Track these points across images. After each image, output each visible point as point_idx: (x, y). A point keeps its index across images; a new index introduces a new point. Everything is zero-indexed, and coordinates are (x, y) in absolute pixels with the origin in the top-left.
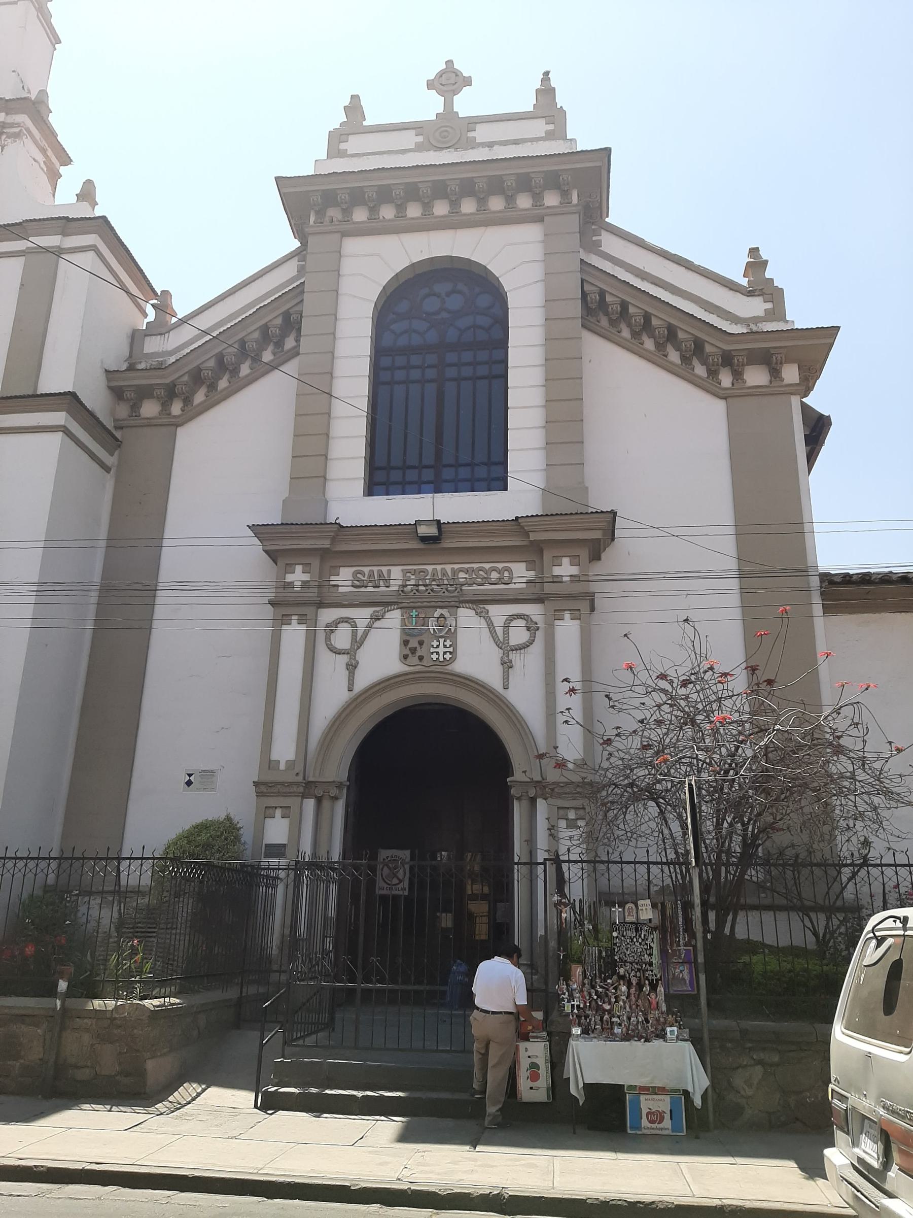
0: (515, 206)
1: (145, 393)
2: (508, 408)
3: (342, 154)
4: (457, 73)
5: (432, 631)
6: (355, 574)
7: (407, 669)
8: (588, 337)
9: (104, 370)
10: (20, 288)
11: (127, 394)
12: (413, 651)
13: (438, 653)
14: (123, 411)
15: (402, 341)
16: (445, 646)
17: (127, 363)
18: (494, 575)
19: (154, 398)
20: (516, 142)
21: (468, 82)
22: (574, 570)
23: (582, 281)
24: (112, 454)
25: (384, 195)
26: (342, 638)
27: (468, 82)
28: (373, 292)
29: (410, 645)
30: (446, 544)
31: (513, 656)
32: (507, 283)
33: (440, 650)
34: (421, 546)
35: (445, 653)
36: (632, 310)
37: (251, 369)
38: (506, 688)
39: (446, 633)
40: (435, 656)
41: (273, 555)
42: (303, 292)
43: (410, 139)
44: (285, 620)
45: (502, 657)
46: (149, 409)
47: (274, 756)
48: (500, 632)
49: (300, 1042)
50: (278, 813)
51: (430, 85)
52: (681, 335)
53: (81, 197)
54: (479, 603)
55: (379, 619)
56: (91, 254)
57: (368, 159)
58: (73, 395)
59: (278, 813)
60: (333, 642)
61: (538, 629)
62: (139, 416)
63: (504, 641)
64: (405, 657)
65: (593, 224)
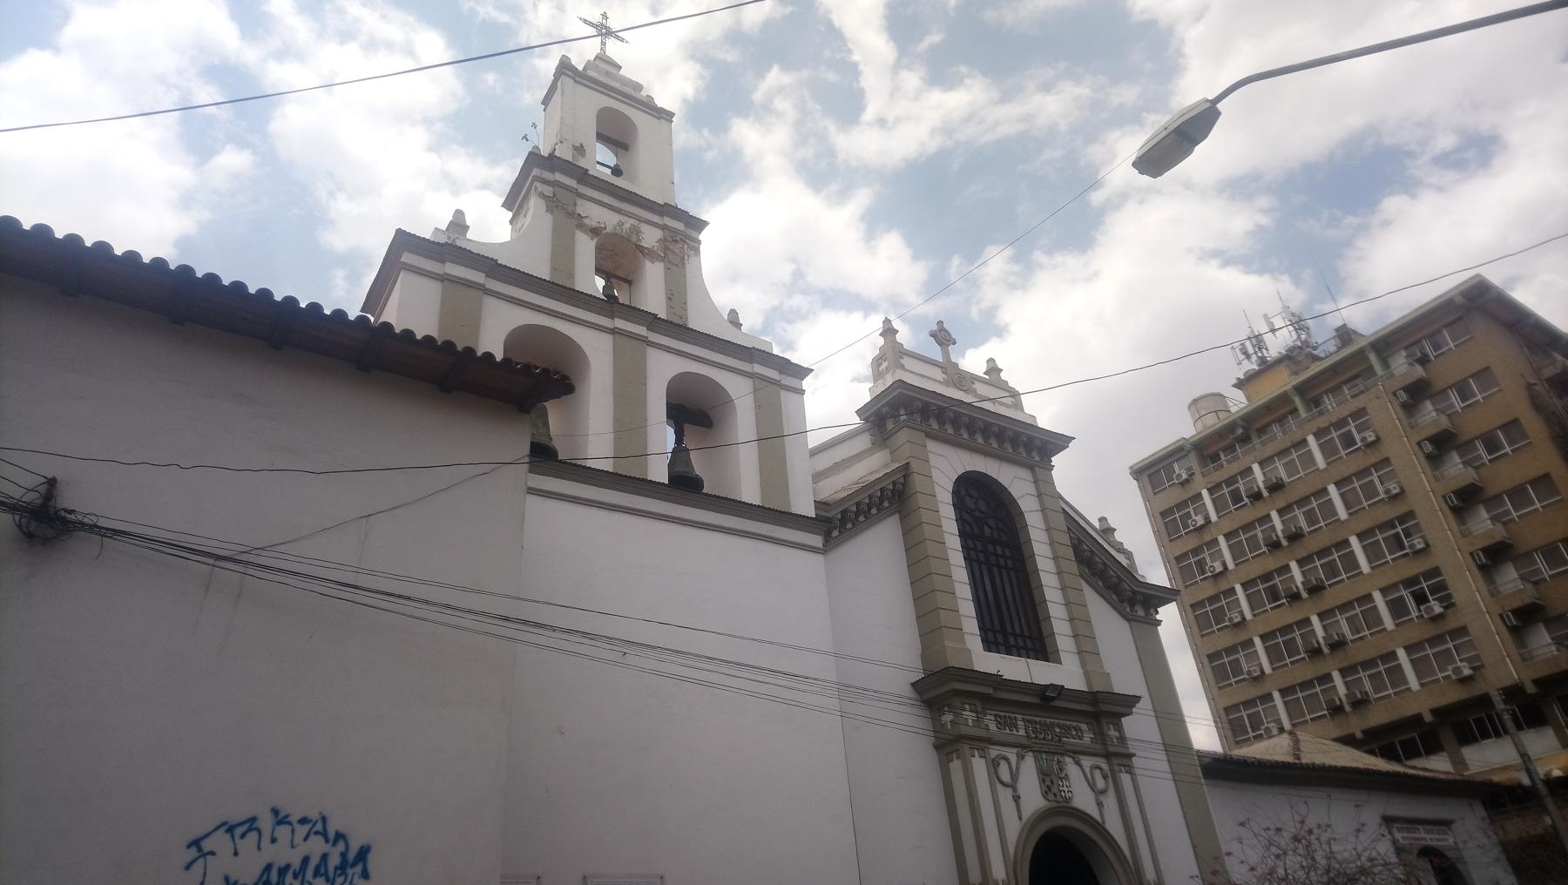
3: (903, 367)
4: (949, 334)
12: (1049, 787)
18: (1074, 733)
22: (1117, 734)
28: (950, 487)
30: (1056, 703)
31: (1102, 798)
38: (1104, 823)
43: (937, 374)
47: (995, 877)
51: (933, 335)
54: (1076, 753)
55: (1022, 759)
60: (1000, 773)
64: (1047, 791)
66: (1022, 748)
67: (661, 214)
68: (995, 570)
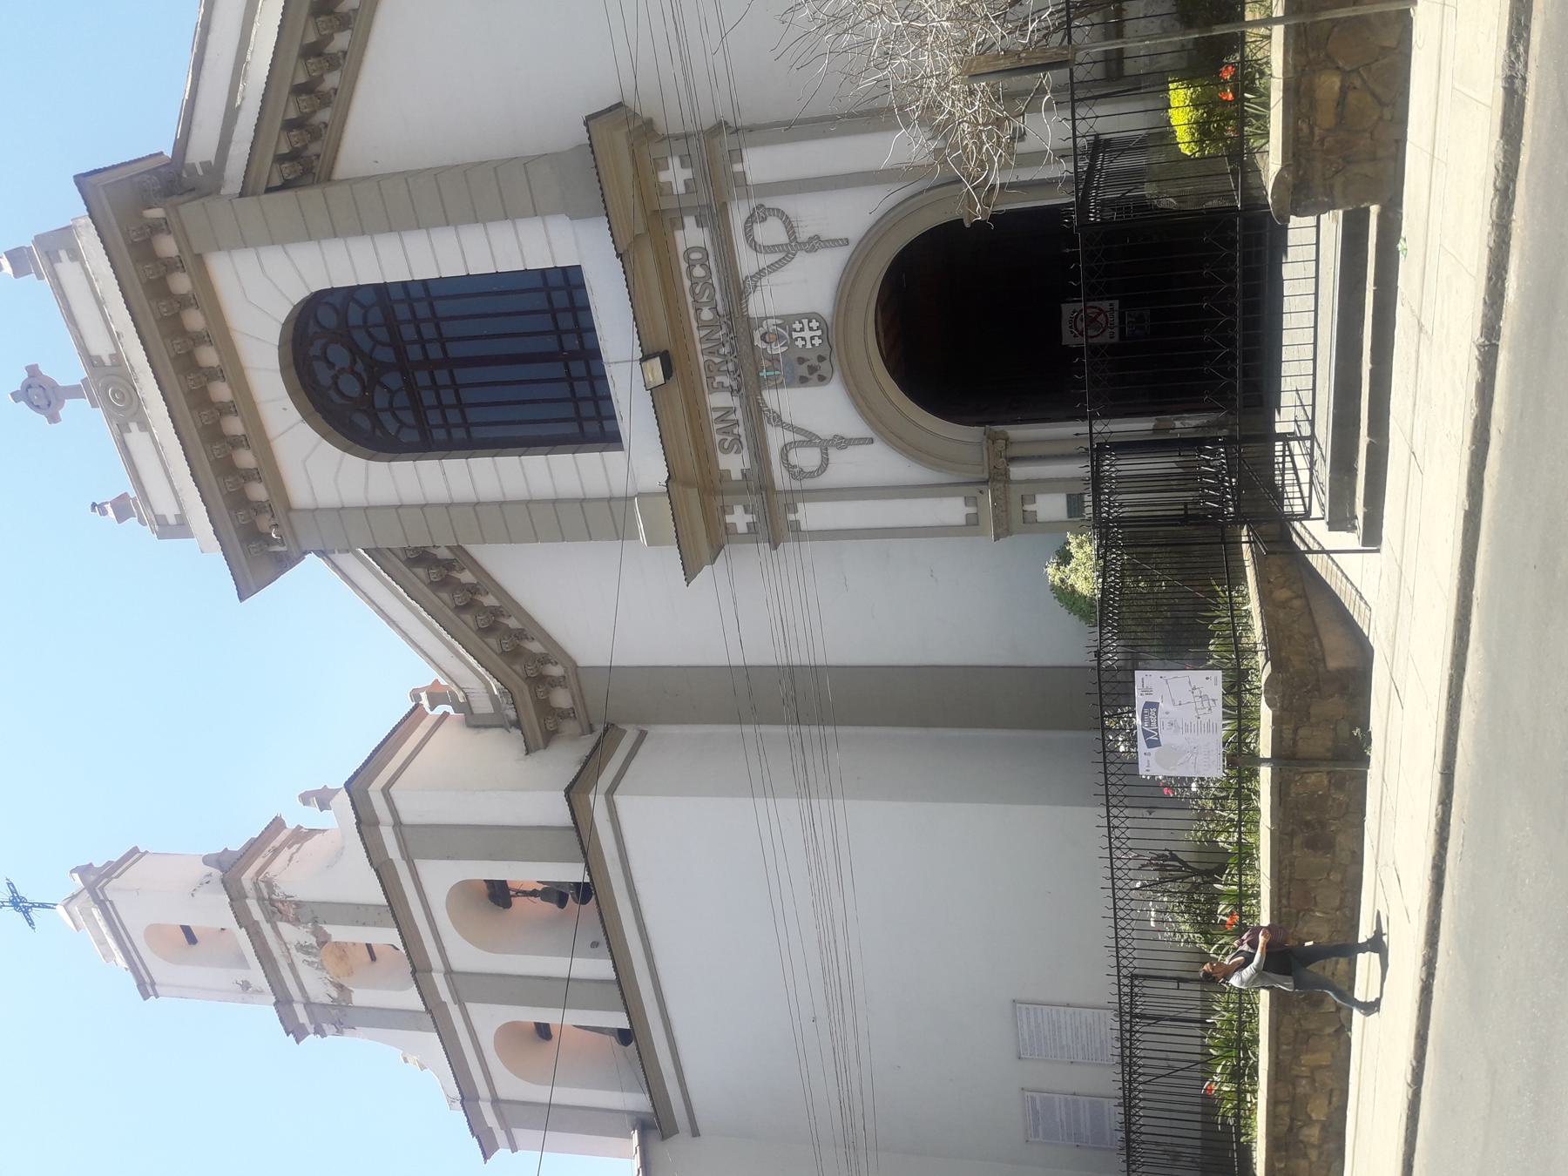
0: (191, 296)
1: (545, 709)
2: (468, 275)
4: (27, 387)
5: (785, 349)
6: (726, 451)
7: (837, 375)
8: (344, 168)
9: (528, 756)
10: (452, 858)
11: (551, 726)
12: (812, 369)
13: (812, 338)
14: (569, 727)
15: (408, 417)
16: (802, 330)
17: (511, 730)
18: (699, 272)
19: (548, 698)
20: (100, 303)
21: (33, 371)
23: (269, 190)
24: (625, 732)
25: (225, 468)
26: (807, 458)
27: (33, 371)
28: (354, 465)
29: (805, 373)
30: (665, 343)
31: (803, 235)
32: (299, 294)
33: (808, 337)
34: (676, 375)
35: (811, 329)
36: (292, 114)
37: (487, 593)
38: (846, 242)
39: (785, 329)
40: (817, 342)
41: (716, 550)
42: (377, 549)
43: (136, 438)
44: (796, 528)
45: (807, 252)
46: (561, 699)
47: (961, 520)
48: (772, 258)
49: (1307, 500)
50: (1029, 508)
51: (54, 419)
52: (312, 37)
53: (324, 806)
54: (737, 291)
55: (779, 417)
56: (393, 791)
57: (181, 490)
58: (568, 792)
59: (1029, 508)
61: (762, 206)
62: (572, 709)
63: (784, 251)
64: (822, 379)
65: (180, 176)
66: (758, 416)
67: (256, 923)
68: (455, 350)
